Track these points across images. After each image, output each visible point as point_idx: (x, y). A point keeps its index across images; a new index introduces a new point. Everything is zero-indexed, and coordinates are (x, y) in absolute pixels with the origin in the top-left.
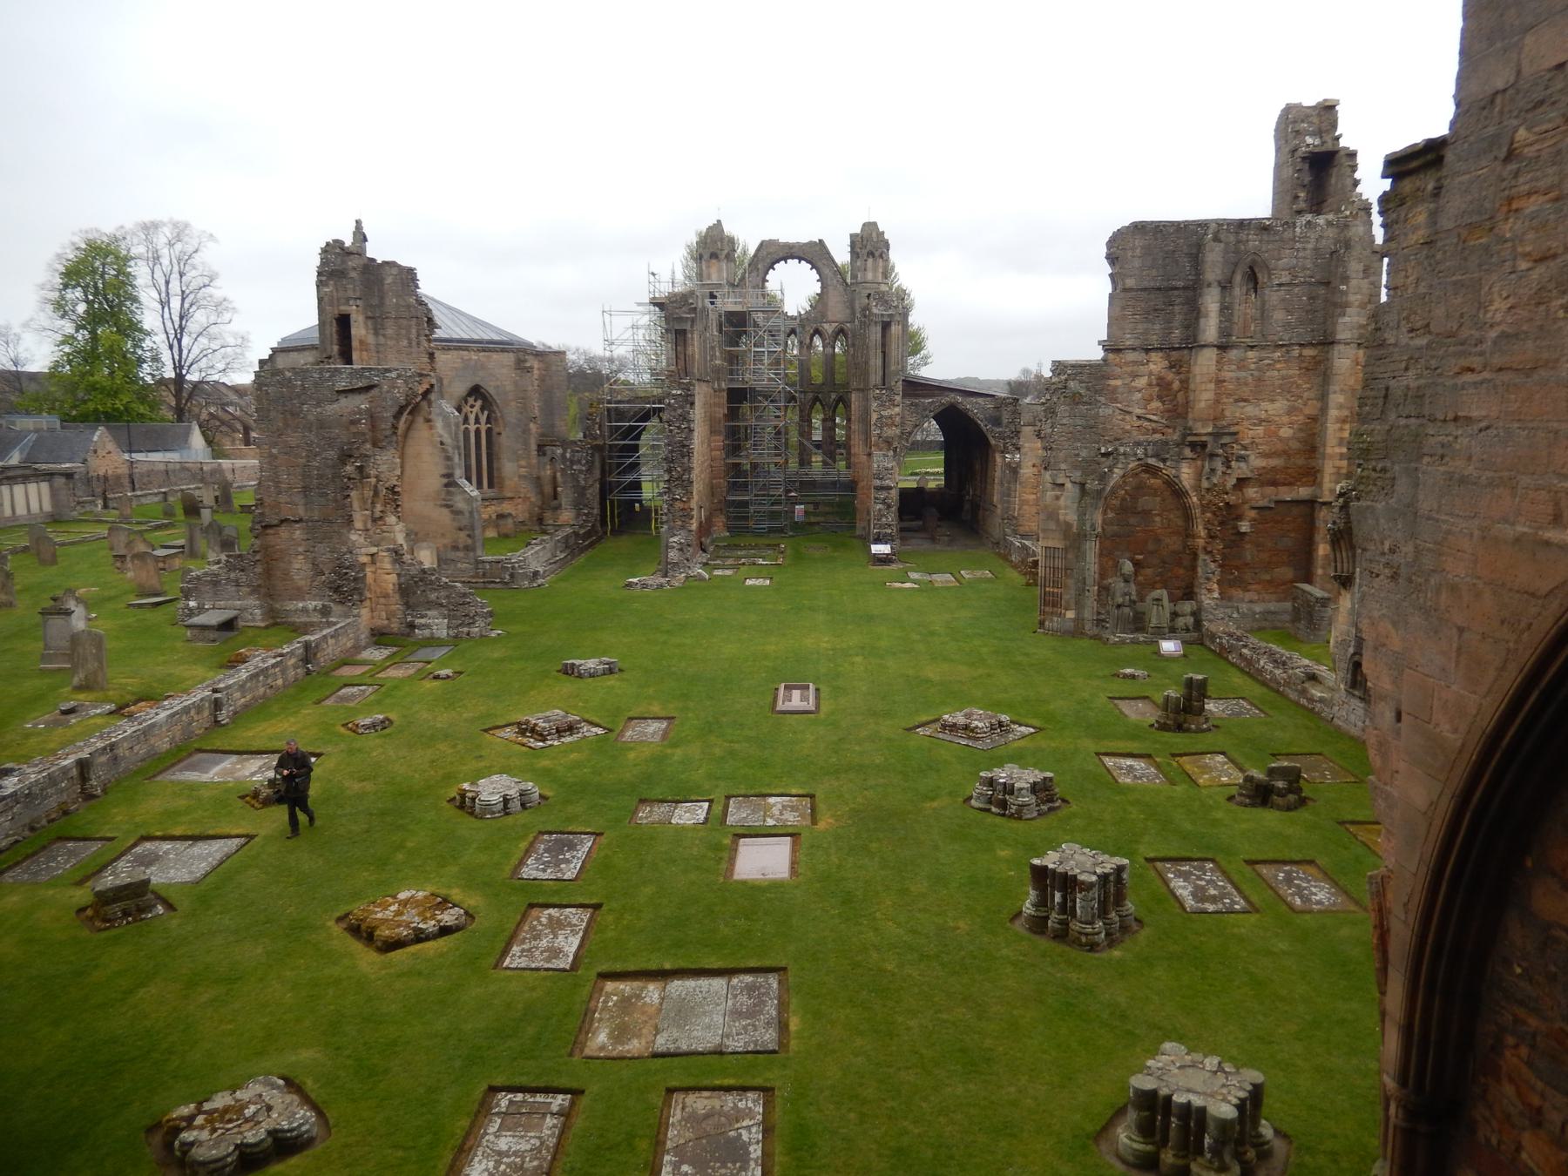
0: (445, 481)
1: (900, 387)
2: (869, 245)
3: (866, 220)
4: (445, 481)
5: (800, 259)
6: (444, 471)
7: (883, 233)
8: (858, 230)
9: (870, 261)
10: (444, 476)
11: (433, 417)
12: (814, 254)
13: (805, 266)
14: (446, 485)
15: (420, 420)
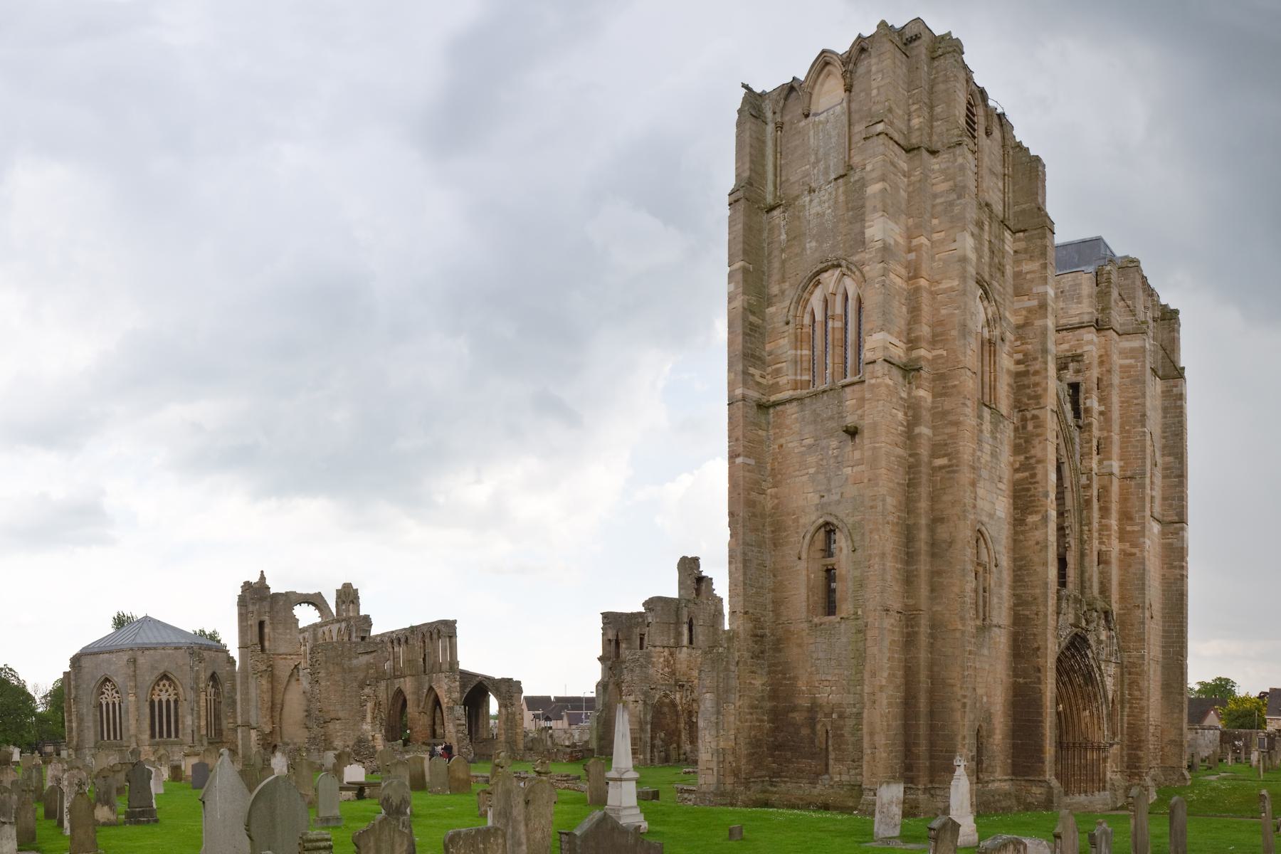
0: (306, 713)
1: (458, 673)
2: (348, 595)
3: (345, 582)
4: (306, 713)
5: (309, 603)
6: (306, 708)
7: (357, 590)
8: (340, 587)
9: (351, 605)
10: (307, 711)
11: (300, 678)
12: (316, 601)
13: (312, 608)
14: (307, 716)
15: (293, 680)
